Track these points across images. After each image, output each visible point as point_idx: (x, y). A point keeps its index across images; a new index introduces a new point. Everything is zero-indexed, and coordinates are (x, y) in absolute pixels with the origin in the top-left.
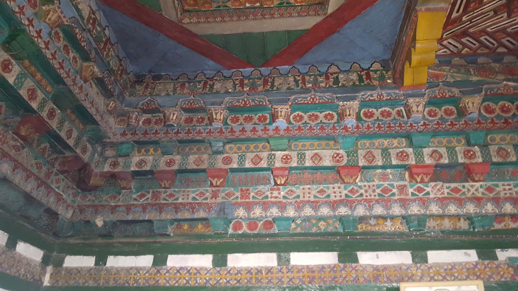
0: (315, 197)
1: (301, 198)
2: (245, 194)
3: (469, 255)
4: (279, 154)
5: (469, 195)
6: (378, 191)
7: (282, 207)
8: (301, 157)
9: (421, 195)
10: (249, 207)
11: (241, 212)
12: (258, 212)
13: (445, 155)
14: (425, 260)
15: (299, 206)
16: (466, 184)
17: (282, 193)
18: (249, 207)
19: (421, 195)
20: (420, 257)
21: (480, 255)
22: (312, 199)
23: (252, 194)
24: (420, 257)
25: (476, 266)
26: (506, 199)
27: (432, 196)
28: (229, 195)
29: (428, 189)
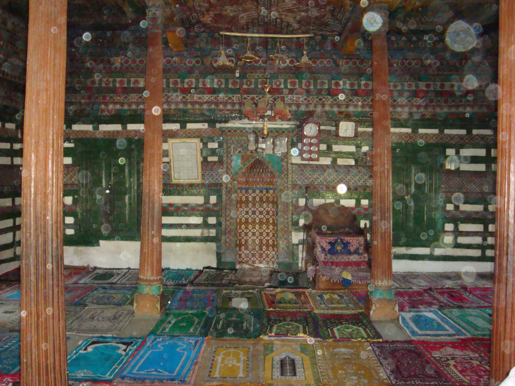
0: (137, 100)
1: (131, 100)
2: (104, 98)
3: (204, 125)
4: (118, 79)
5: (205, 100)
6: (166, 98)
7: (122, 104)
8: (129, 82)
9: (184, 100)
10: (106, 104)
11: (103, 107)
12: (111, 107)
13: (194, 83)
14: (185, 127)
15: (130, 105)
16: (205, 96)
17: (122, 98)
18: (106, 104)
19: (184, 100)
20: (183, 126)
21: (209, 126)
22: (136, 101)
23: (108, 98)
24: (183, 126)
25: (206, 130)
26: (221, 103)
27: (189, 100)
28: (97, 98)
29: (188, 97)
